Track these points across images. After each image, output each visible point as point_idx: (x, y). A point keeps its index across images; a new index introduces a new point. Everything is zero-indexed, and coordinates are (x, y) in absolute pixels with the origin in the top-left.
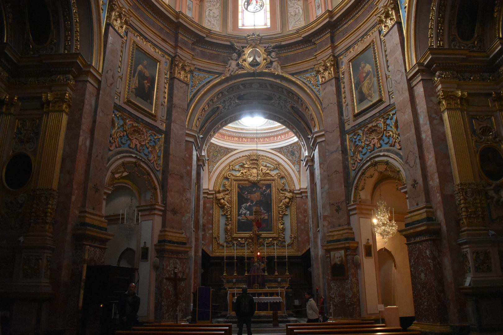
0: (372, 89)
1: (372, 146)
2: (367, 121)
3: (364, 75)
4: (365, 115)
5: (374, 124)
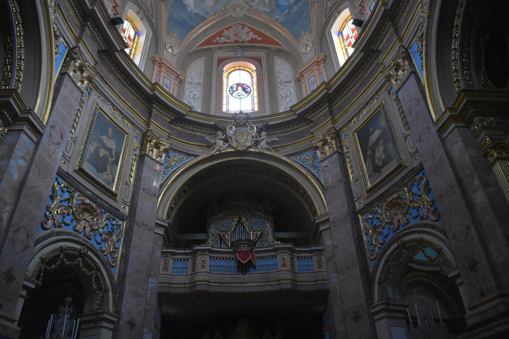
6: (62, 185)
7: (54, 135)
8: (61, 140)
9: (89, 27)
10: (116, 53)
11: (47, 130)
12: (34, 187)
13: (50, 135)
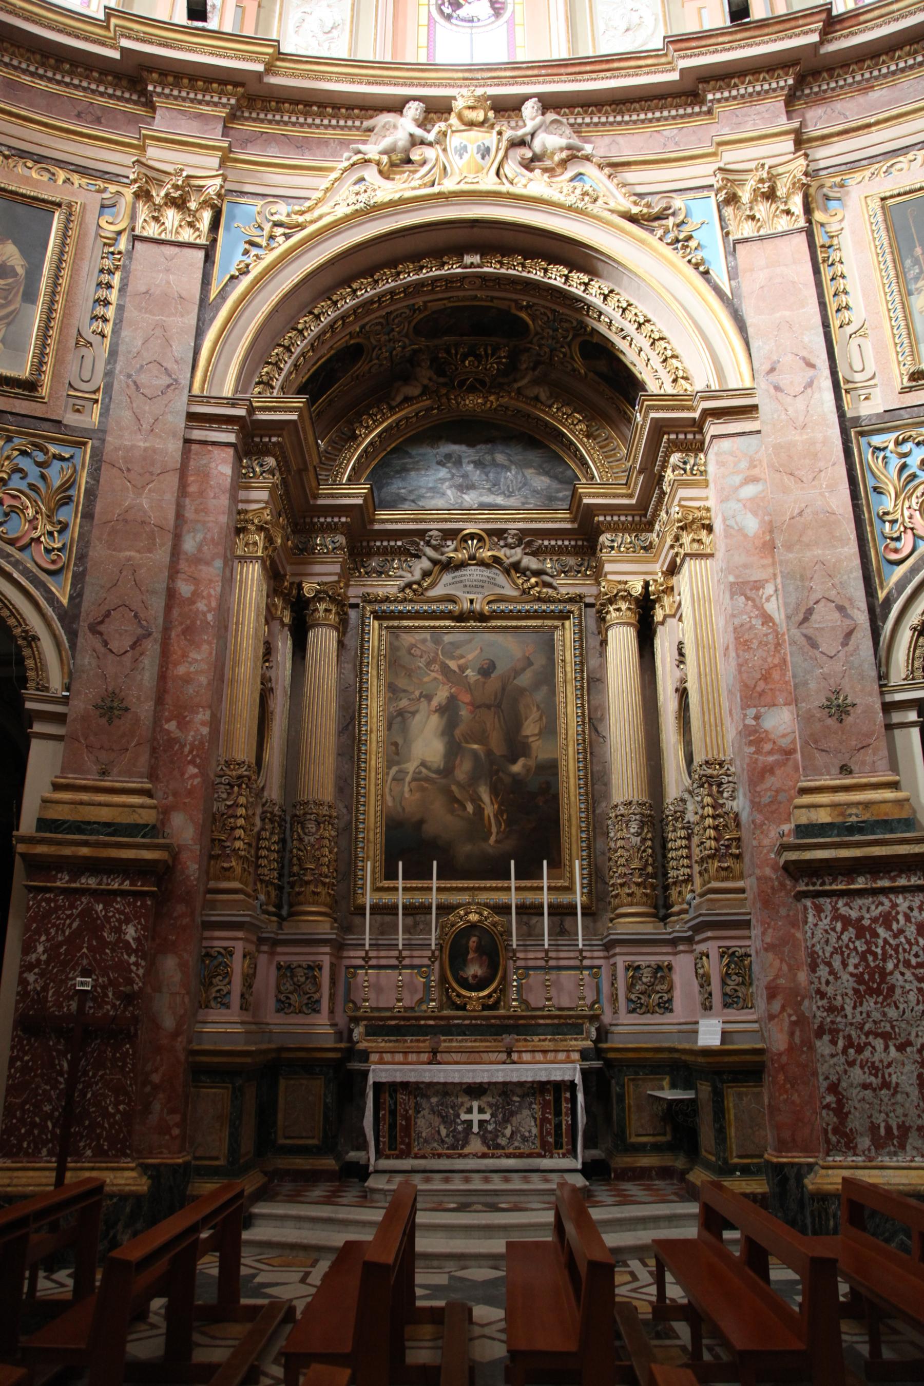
6: (891, 446)
7: (784, 379)
8: (811, 372)
9: (719, 101)
10: (823, 50)
11: (763, 385)
12: (800, 514)
13: (777, 388)
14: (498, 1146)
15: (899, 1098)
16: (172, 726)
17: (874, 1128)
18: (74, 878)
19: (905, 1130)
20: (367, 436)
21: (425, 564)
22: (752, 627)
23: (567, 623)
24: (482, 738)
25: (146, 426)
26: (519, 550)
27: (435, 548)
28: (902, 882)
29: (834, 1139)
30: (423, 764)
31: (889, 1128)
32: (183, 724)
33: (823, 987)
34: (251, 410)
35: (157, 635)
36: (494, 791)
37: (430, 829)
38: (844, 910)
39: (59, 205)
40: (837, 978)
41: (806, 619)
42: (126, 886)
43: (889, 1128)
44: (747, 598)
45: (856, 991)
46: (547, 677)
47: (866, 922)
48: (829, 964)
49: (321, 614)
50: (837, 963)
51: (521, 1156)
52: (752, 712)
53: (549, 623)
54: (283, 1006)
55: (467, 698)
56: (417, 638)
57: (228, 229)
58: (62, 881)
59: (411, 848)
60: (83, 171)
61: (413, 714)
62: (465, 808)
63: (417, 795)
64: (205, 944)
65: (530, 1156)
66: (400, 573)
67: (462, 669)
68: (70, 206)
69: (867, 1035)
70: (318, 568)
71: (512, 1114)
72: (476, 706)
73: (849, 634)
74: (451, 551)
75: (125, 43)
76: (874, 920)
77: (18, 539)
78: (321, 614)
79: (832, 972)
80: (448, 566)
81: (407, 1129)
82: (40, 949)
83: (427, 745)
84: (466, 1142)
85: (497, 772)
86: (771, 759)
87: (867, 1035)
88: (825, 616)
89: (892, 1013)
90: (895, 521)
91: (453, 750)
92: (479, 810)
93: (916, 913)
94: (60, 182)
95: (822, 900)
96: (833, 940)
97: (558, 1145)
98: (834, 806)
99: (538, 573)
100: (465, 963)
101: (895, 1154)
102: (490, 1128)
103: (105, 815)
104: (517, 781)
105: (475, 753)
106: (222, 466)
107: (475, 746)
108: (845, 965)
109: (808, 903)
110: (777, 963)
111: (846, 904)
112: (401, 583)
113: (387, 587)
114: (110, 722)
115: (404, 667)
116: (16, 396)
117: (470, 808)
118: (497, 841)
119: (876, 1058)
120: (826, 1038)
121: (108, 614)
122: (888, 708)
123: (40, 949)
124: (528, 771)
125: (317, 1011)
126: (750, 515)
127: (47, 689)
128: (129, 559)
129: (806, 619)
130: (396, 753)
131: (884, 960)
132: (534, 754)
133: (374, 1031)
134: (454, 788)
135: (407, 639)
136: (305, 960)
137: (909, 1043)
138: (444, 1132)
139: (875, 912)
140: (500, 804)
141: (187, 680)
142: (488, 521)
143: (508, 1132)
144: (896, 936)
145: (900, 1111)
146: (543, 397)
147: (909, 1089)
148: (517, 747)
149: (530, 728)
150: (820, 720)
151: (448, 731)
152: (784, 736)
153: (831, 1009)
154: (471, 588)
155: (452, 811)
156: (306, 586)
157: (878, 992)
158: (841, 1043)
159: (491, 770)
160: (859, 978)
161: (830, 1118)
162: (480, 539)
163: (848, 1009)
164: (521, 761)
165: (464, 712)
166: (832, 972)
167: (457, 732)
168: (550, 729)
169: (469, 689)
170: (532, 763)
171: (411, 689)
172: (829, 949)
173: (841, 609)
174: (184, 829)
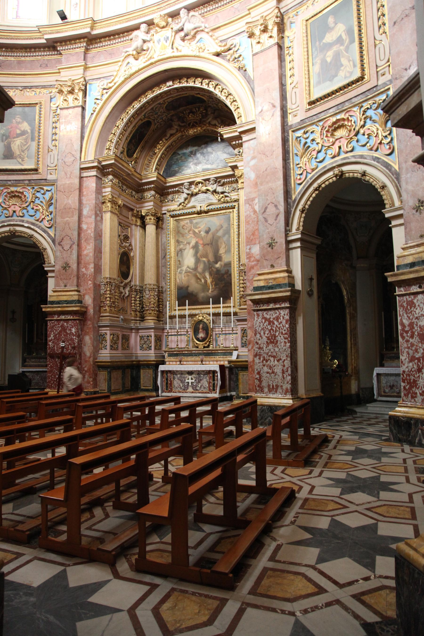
0: (26, 152)
1: (11, 212)
2: (10, 183)
3: (18, 132)
4: (9, 175)
5: (19, 189)
12: (266, 170)
14: (197, 390)
15: (277, 376)
16: (84, 270)
17: (269, 386)
18: (58, 317)
19: (277, 386)
20: (159, 152)
21: (185, 196)
22: (250, 216)
23: (234, 210)
24: (206, 256)
25: (68, 176)
26: (215, 185)
27: (188, 189)
28: (283, 305)
29: (258, 389)
30: (188, 267)
31: (273, 386)
32: (87, 269)
33: (258, 341)
34: (99, 162)
35: (76, 243)
36: (211, 274)
37: (190, 289)
38: (265, 316)
39: (37, 104)
40: (262, 338)
41: (265, 211)
42: (72, 318)
43: (273, 386)
44: (250, 205)
45: (267, 342)
46: (228, 232)
47: (271, 320)
48: (260, 334)
49: (148, 220)
50: (262, 333)
51: (203, 393)
52: (248, 247)
53: (228, 211)
54: (142, 348)
55: (201, 242)
56: (185, 222)
57: (89, 95)
58: (56, 317)
59: (186, 297)
60: (44, 87)
61: (184, 249)
62: (201, 281)
63: (186, 278)
64: (100, 332)
65: (206, 393)
66: (178, 199)
67: (200, 232)
68: (41, 103)
69: (269, 356)
70: (146, 204)
71: (201, 380)
72: (204, 245)
73: (277, 216)
74: (194, 189)
75: (47, 37)
76: (274, 319)
77: (39, 219)
78: (148, 220)
79: (261, 336)
80: (192, 195)
81: (171, 384)
82: (52, 336)
83: (189, 260)
84: (188, 388)
85: (211, 268)
86: (253, 263)
87: (269, 356)
88: (271, 210)
89: (277, 349)
90: (301, 167)
91: (198, 261)
92: (206, 281)
93: (286, 316)
94: (38, 93)
95: (259, 312)
96: (262, 326)
97: (214, 390)
98: (265, 280)
99: (223, 193)
100: (198, 333)
101: (274, 394)
102: (194, 384)
103: (65, 298)
104: (218, 270)
105: (204, 262)
106: (91, 184)
107: (204, 259)
108: (264, 334)
109: (255, 313)
110: (251, 333)
111: (266, 314)
112: (178, 204)
113: (173, 206)
114: (66, 271)
115: (181, 233)
116: (33, 174)
117: (203, 281)
118: (212, 292)
119: (271, 364)
120: (258, 357)
121: (63, 239)
122: (288, 242)
123: (52, 336)
124: (221, 266)
125: (151, 349)
126: (252, 172)
127: (50, 263)
128: (67, 221)
129: (265, 211)
130: (179, 264)
131: (276, 332)
132: (223, 260)
133: (170, 355)
134: (198, 274)
135: (182, 223)
136: (146, 334)
137: (280, 359)
138: (181, 385)
139: (274, 316)
140: (213, 279)
141: (87, 255)
142: (204, 176)
143: (200, 386)
144: (279, 324)
145: (276, 381)
146: (217, 124)
147: (279, 374)
148: (218, 258)
149: (222, 251)
150: (266, 249)
151: (196, 254)
152: (258, 255)
153: (260, 348)
154: (200, 202)
155: (197, 282)
156: (142, 211)
157: (273, 342)
158: (262, 359)
159: (209, 267)
160: (268, 338)
161: (257, 382)
162: (202, 183)
163: (264, 348)
164: (219, 263)
165: (201, 247)
166: (261, 336)
167: (198, 255)
168: (228, 251)
169: (202, 239)
170: (222, 263)
171: (183, 241)
172: (260, 329)
173: (276, 206)
174: (89, 300)
